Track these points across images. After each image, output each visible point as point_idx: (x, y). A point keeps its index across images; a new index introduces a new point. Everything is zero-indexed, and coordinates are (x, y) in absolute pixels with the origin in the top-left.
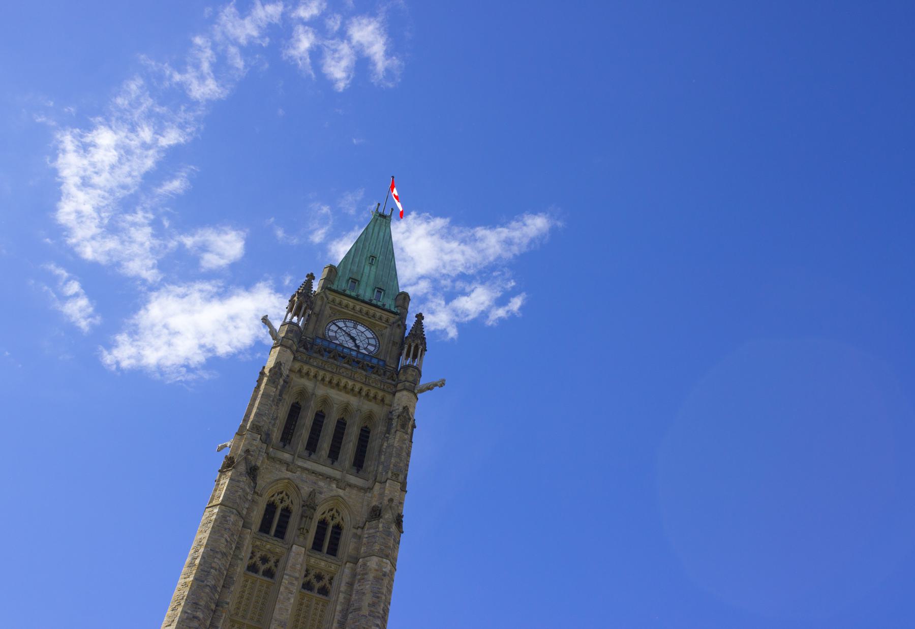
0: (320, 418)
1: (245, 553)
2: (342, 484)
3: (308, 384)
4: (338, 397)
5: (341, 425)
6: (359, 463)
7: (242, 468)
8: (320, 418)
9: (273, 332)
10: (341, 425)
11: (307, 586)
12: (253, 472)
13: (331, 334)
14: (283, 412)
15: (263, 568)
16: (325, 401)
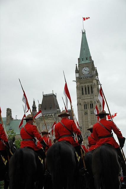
0: (86, 88)
1: (84, 114)
2: (91, 98)
3: (82, 85)
4: (87, 85)
5: (88, 88)
6: (92, 92)
7: (79, 104)
8: (86, 88)
9: (75, 81)
10: (88, 88)
11: (91, 113)
12: (80, 104)
13: (83, 72)
14: (81, 92)
15: (86, 114)
16: (85, 86)
